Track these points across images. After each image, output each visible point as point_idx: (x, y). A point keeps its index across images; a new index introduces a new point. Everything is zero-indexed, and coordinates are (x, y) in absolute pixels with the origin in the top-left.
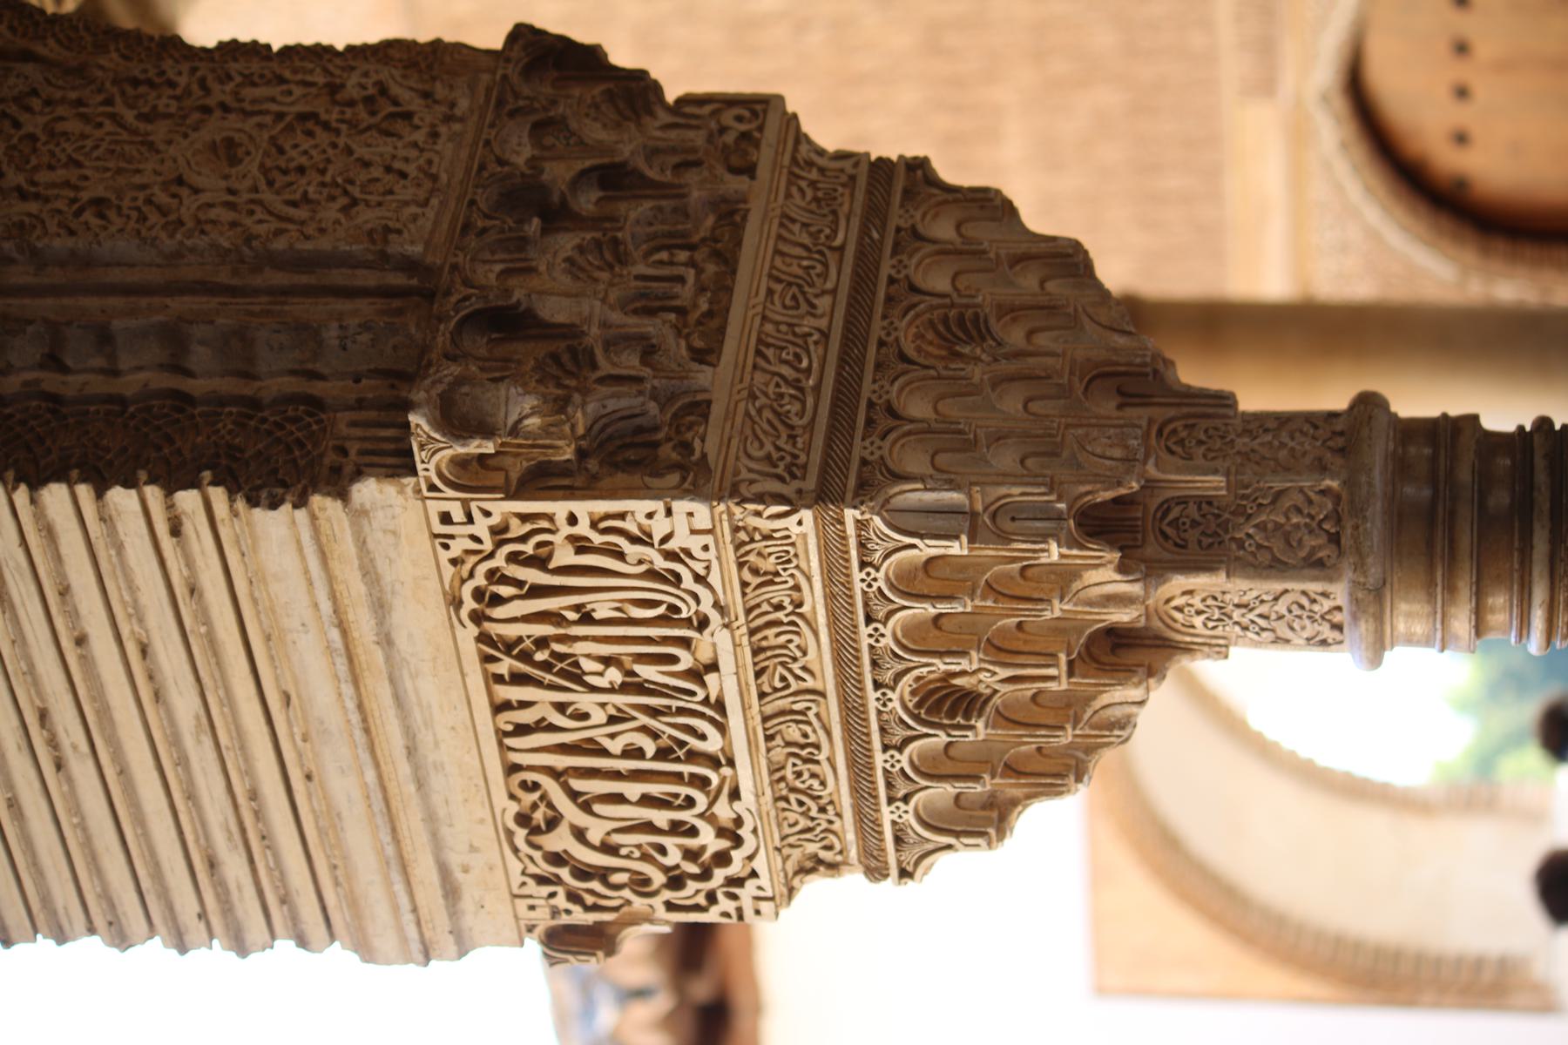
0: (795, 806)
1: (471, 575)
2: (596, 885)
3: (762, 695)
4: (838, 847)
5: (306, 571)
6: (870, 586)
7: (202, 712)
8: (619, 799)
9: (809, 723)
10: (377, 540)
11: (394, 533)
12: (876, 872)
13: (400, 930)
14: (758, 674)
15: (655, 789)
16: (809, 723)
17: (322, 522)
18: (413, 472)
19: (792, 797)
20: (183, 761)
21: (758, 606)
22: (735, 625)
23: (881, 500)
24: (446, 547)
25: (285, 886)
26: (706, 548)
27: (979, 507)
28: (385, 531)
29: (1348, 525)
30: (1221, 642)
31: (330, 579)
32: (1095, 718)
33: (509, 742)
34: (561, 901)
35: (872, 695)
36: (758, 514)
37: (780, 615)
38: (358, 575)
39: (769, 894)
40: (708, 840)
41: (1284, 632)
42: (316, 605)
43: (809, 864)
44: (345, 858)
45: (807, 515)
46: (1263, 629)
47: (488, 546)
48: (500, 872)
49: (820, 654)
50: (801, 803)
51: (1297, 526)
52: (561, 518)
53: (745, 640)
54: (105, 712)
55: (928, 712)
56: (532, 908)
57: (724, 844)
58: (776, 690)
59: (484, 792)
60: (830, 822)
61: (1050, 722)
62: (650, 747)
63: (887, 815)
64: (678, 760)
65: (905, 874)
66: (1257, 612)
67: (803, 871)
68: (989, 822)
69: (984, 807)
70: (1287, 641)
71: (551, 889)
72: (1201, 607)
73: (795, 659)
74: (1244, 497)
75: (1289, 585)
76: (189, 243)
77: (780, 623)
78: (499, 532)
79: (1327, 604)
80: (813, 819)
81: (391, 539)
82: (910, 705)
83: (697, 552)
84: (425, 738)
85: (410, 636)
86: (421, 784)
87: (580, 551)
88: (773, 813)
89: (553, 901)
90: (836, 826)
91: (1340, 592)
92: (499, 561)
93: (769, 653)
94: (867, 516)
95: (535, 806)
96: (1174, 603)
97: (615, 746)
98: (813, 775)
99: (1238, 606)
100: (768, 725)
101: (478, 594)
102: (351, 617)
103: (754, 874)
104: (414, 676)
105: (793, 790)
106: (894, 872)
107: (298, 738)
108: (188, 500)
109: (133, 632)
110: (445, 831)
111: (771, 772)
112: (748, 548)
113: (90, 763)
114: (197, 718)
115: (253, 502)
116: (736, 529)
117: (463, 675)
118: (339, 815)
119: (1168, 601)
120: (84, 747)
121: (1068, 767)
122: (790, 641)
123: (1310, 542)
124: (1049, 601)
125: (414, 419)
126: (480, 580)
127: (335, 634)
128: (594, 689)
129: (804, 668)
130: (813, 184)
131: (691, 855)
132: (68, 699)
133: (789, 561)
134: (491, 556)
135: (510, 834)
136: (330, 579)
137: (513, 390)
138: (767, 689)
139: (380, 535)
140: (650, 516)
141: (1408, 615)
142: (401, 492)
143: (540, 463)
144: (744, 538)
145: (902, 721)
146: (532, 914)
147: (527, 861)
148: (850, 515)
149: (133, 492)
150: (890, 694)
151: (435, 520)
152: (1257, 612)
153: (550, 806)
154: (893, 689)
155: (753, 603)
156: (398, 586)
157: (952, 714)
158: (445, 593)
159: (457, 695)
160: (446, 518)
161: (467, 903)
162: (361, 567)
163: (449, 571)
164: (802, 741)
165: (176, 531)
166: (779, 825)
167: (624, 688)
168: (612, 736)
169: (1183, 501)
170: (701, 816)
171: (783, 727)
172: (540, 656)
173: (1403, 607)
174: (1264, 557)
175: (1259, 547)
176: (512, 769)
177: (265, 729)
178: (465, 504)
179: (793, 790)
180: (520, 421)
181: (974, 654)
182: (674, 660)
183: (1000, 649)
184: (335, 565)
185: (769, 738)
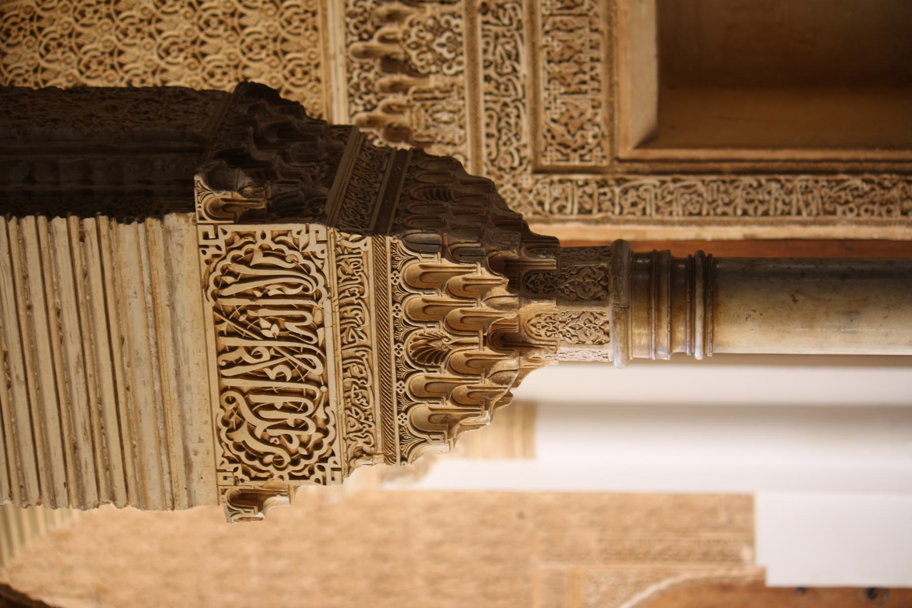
0: (354, 415)
1: (214, 270)
2: (256, 463)
3: (343, 344)
4: (373, 442)
5: (140, 262)
6: (395, 281)
7: (81, 354)
8: (271, 407)
9: (363, 365)
10: (174, 249)
11: (181, 245)
12: (389, 459)
13: (162, 486)
14: (342, 331)
15: (289, 399)
16: (363, 365)
17: (150, 233)
18: (194, 210)
19: (353, 408)
20: (68, 382)
21: (344, 291)
22: (334, 299)
23: (403, 234)
24: (204, 252)
25: (109, 460)
26: (323, 252)
27: (446, 243)
28: (177, 244)
29: (612, 281)
30: (553, 343)
31: (151, 267)
32: (495, 377)
33: (224, 372)
34: (239, 474)
35: (393, 347)
36: (347, 239)
37: (353, 298)
38: (163, 264)
39: (339, 466)
40: (312, 434)
41: (582, 338)
42: (142, 283)
43: (358, 454)
44: (140, 440)
45: (369, 239)
46: (573, 336)
47: (223, 252)
48: (211, 455)
49: (370, 324)
50: (357, 414)
51: (588, 283)
52: (258, 236)
53: (337, 309)
54: (34, 352)
55: (418, 359)
56: (225, 478)
57: (320, 435)
58: (350, 343)
59: (209, 404)
60: (370, 426)
61: (475, 373)
62: (289, 374)
63: (397, 423)
64: (301, 382)
65: (403, 459)
66: (570, 325)
67: (356, 457)
68: (444, 428)
69: (442, 422)
70: (584, 343)
71: (236, 465)
72: (544, 323)
73: (359, 326)
74: (564, 271)
75: (584, 309)
76: (96, 130)
77: (353, 304)
78: (229, 243)
79: (602, 319)
80: (362, 424)
81: (179, 249)
82: (410, 354)
83: (319, 255)
84: (184, 369)
85: (183, 306)
86: (180, 395)
87: (265, 255)
88: (344, 416)
89: (236, 474)
90: (372, 430)
91: (608, 313)
92: (228, 262)
93: (347, 321)
94: (396, 241)
95: (232, 415)
96: (532, 322)
97: (272, 374)
98: (363, 397)
99: (561, 322)
100: (345, 362)
101: (216, 283)
102: (158, 291)
103: (333, 454)
104: (183, 331)
105: (353, 405)
106: (398, 458)
107: (125, 364)
108: (89, 223)
109: (54, 304)
110: (188, 427)
111: (345, 392)
112: (341, 257)
113: (24, 387)
114: (78, 357)
115: (119, 221)
116: (337, 246)
117: (205, 330)
118: (140, 412)
119: (529, 321)
120: (22, 378)
121: (482, 402)
122: (357, 314)
123: (595, 290)
124: (476, 299)
125: (197, 178)
126: (218, 273)
127: (149, 298)
128: (266, 338)
129: (362, 331)
130: (371, 154)
131: (303, 445)
132: (18, 346)
133: (359, 268)
134: (225, 258)
135: (219, 430)
136: (151, 267)
137: (241, 172)
138: (345, 342)
139: (175, 246)
140: (299, 233)
141: (640, 336)
142: (187, 221)
143: (251, 210)
144: (340, 253)
145: (407, 363)
146: (225, 483)
147: (225, 447)
148: (389, 239)
149: (64, 220)
150: (402, 347)
151: (201, 236)
152: (570, 325)
153: (240, 414)
154: (403, 343)
155: (342, 289)
156: (180, 277)
157: (429, 361)
158: (201, 282)
159: (201, 342)
160: (206, 236)
161: (195, 476)
162: (165, 260)
163: (204, 267)
164: (359, 376)
165: (82, 239)
166: (347, 425)
167: (280, 338)
168: (271, 367)
169: (536, 272)
170: (310, 416)
171: (351, 365)
172: (242, 319)
173: (636, 331)
174: (573, 296)
175: (571, 292)
176: (223, 390)
177: (110, 363)
178: (216, 226)
179: (353, 405)
180: (243, 188)
181: (441, 322)
182: (303, 319)
183: (452, 329)
184: (153, 259)
185: (345, 370)
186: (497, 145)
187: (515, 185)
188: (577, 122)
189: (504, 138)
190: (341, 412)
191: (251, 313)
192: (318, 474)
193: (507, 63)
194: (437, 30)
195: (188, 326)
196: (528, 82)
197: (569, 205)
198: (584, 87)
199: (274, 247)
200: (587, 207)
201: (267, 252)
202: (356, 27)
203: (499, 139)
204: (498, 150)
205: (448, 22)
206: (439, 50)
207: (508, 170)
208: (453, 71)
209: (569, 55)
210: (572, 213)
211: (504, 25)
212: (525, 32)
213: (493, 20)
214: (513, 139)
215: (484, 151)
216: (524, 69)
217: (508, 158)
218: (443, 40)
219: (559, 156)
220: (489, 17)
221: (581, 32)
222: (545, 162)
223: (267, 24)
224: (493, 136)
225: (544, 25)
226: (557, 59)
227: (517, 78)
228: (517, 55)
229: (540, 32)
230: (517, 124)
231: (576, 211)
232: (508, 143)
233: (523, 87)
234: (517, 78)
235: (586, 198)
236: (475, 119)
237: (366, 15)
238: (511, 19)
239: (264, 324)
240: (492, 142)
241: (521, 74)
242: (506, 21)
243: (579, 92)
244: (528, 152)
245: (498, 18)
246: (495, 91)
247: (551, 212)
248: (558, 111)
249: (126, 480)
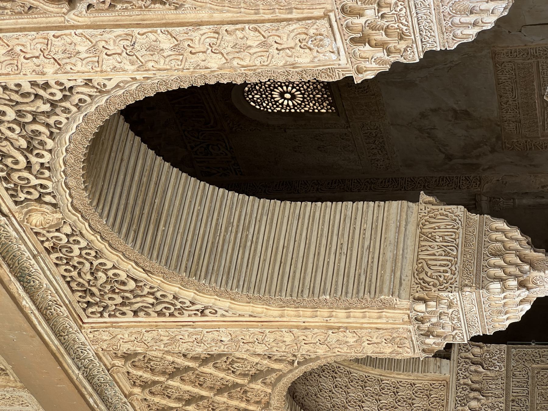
2: (426, 285)
34: (419, 289)
45: (478, 215)
84: (405, 251)
120: (345, 253)
127: (398, 224)
159: (413, 243)
161: (402, 288)
163: (419, 219)
184: (402, 213)
190: (461, 267)
191: (433, 234)
192: (450, 289)
195: (410, 238)
199: (445, 213)
201: (441, 214)
220: (515, 404)
223: (423, 403)
239: (437, 237)
249: (376, 288)
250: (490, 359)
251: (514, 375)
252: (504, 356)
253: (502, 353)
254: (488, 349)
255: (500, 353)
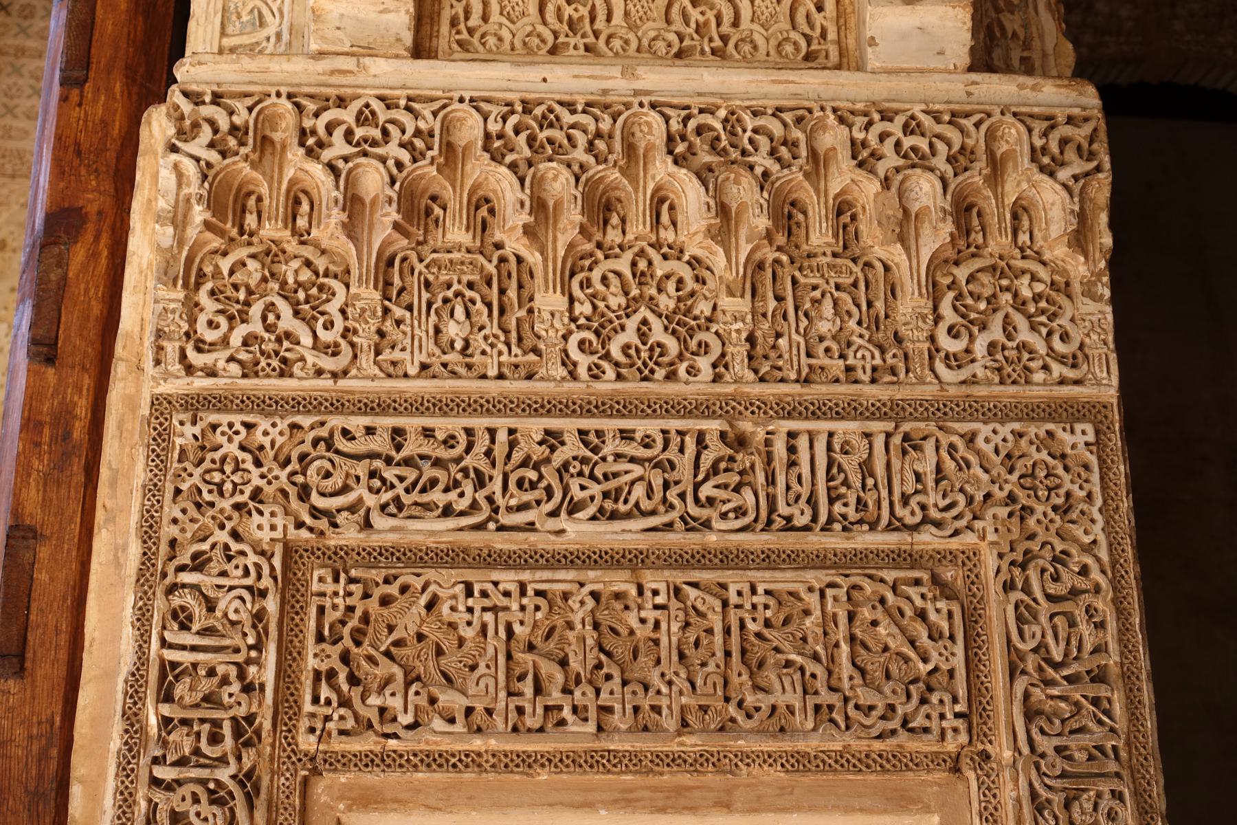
186: (372, 456)
187: (256, 494)
188: (427, 666)
189: (390, 474)
193: (595, 489)
194: (682, 322)
196: (540, 541)
197: (188, 639)
198: (528, 688)
200: (180, 690)
202: (699, 131)
203: (389, 461)
204: (358, 457)
205: (704, 348)
206: (632, 324)
207: (300, 479)
208: (575, 354)
209: (615, 653)
210: (164, 643)
211: (697, 486)
212: (677, 539)
213: (707, 460)
214: (386, 496)
215: (357, 423)
216: (579, 531)
217: (337, 481)
218: (658, 333)
219: (331, 616)
220: (716, 450)
221: (681, 683)
222: (318, 579)
224: (398, 448)
225: (695, 585)
226: (603, 616)
227: (554, 514)
228: (614, 516)
229: (679, 577)
230: (427, 507)
231: (171, 655)
232: (377, 483)
233: (530, 527)
234: (554, 514)
235: (206, 685)
236: (442, 407)
237: (735, 154)
238: (711, 501)
240: (381, 443)
241: (563, 522)
242: (706, 491)
243: (514, 676)
244: (349, 535)
245: (715, 470)
246: (517, 456)
247: (171, 589)
248: (461, 617)
250: (1007, 297)
251: (911, 443)
252: (1039, 376)
253: (1057, 369)
254: (1077, 288)
255: (1061, 359)
